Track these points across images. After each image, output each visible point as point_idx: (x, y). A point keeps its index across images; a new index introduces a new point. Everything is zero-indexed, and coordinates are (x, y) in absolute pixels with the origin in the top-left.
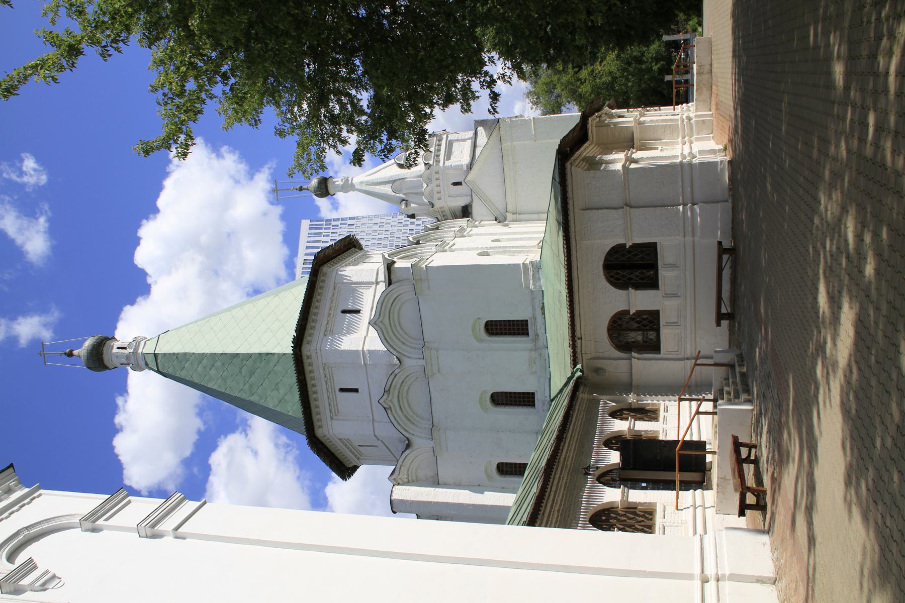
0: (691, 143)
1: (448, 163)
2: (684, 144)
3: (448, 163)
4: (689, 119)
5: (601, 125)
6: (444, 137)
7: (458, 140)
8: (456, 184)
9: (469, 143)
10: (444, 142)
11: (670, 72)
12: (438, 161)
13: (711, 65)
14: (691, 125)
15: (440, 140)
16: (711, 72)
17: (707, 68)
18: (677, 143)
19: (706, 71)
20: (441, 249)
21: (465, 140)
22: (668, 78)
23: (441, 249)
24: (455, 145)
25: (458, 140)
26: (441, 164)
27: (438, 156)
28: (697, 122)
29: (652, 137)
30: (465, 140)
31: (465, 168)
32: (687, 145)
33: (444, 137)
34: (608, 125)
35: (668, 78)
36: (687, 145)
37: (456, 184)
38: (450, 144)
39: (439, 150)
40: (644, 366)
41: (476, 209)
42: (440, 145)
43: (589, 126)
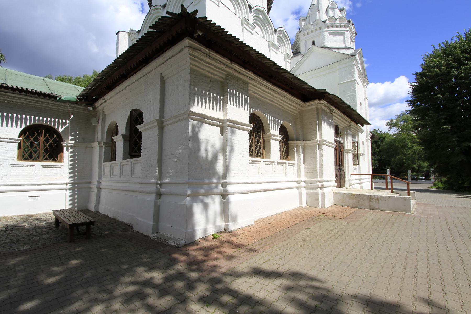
0: (298, 188)
1: (327, 34)
2: (298, 182)
3: (327, 34)
4: (322, 188)
5: (319, 112)
6: (348, 29)
7: (344, 38)
8: (313, 43)
9: (343, 46)
10: (344, 29)
11: (412, 172)
12: (328, 27)
13: (378, 209)
14: (316, 188)
15: (345, 26)
16: (371, 208)
17: (375, 205)
18: (299, 175)
19: (372, 204)
20: (243, 21)
21: (345, 42)
22: (409, 171)
23: (243, 21)
24: (341, 37)
25: (344, 38)
26: (326, 29)
27: (332, 27)
28: (317, 194)
29: (307, 156)
30: (345, 42)
31: (323, 45)
32: (297, 185)
33: (348, 29)
34: (318, 118)
35: (409, 171)
36: (297, 185)
37: (313, 43)
38: (342, 34)
39: (337, 27)
40: (97, 150)
41: (298, 58)
42: (341, 27)
43: (317, 101)
